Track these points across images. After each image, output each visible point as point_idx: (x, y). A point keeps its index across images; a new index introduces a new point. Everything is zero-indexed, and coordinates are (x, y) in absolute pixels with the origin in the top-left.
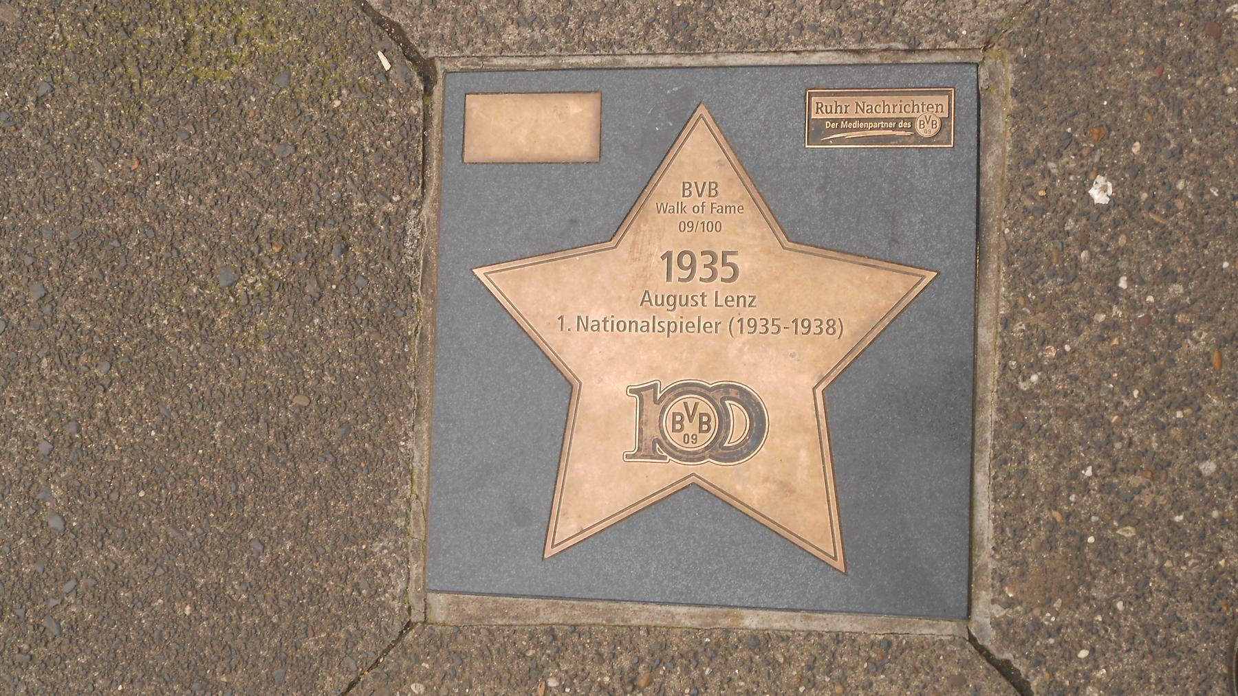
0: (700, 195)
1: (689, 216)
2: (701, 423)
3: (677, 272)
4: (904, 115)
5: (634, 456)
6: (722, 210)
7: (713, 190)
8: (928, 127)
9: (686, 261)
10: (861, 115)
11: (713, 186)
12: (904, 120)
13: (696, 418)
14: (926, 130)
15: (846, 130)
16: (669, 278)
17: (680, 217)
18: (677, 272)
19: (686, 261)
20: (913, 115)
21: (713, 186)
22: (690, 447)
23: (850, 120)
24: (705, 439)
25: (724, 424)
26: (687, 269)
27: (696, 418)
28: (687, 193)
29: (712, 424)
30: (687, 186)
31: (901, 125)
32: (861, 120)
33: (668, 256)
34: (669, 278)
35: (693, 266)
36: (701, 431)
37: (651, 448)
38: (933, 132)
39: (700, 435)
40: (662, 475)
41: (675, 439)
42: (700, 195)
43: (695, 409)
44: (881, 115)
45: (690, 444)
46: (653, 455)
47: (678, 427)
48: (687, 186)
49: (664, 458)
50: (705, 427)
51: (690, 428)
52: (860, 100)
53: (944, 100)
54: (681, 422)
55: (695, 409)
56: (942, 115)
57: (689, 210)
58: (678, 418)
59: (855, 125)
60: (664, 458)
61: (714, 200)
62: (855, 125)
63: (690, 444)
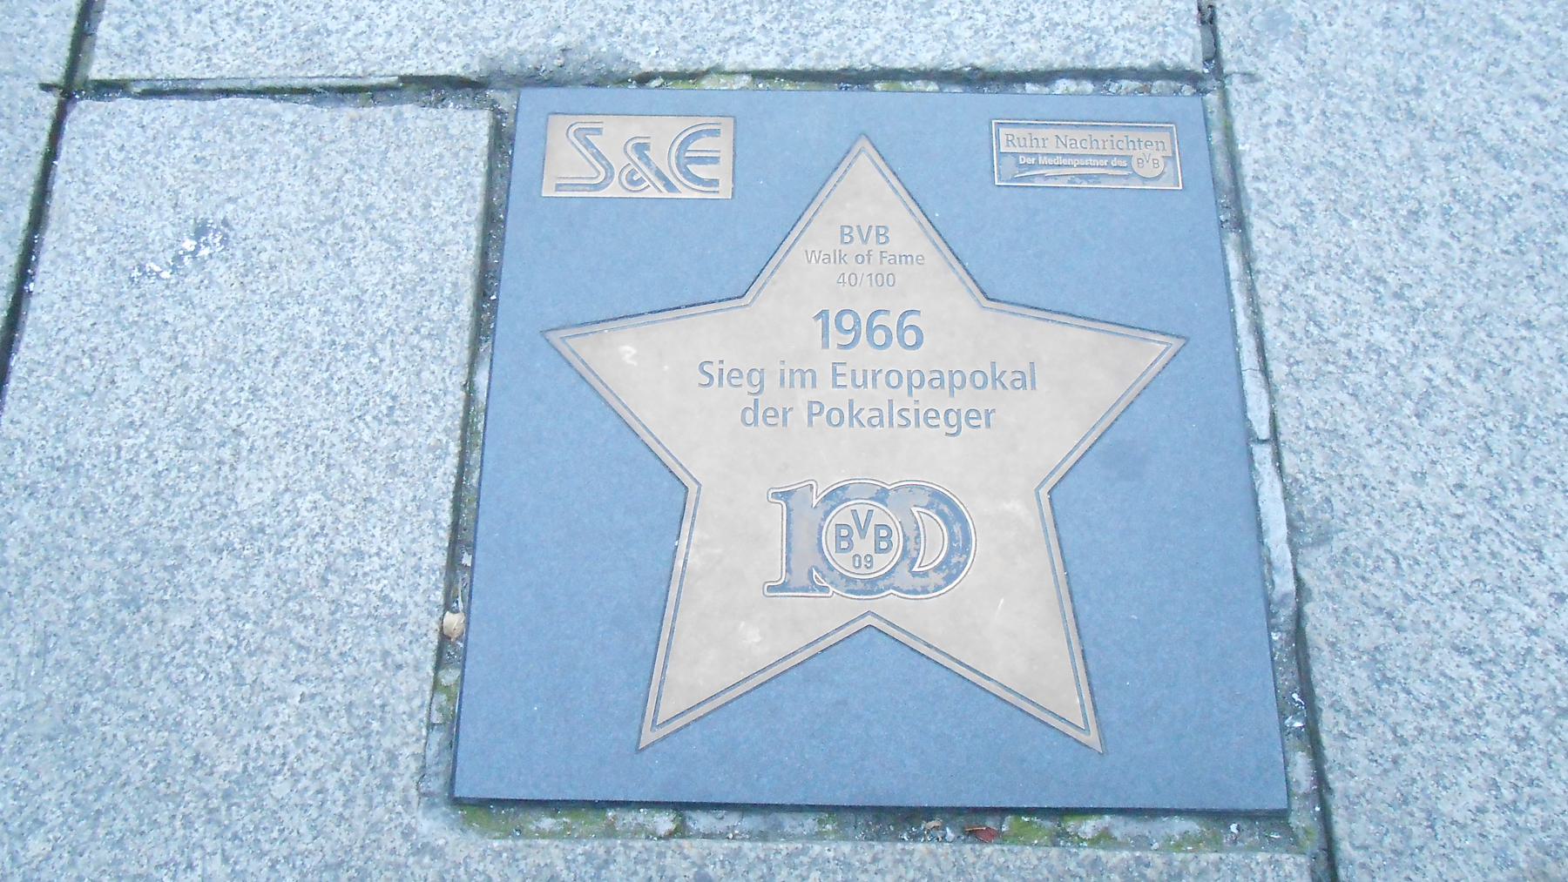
0: (865, 242)
2: (878, 539)
3: (835, 337)
5: (783, 587)
6: (894, 259)
7: (882, 233)
9: (848, 322)
11: (882, 231)
13: (871, 530)
16: (826, 345)
18: (835, 337)
19: (848, 322)
22: (863, 574)
24: (883, 563)
25: (913, 538)
26: (849, 331)
27: (871, 530)
28: (847, 239)
29: (894, 539)
30: (847, 231)
33: (823, 315)
34: (826, 345)
35: (856, 329)
36: (878, 550)
37: (800, 578)
39: (876, 557)
40: (829, 613)
41: (843, 562)
42: (865, 242)
43: (867, 521)
45: (863, 570)
46: (811, 587)
47: (844, 545)
48: (847, 231)
49: (823, 589)
50: (883, 545)
51: (864, 546)
54: (848, 538)
55: (867, 521)
57: (850, 259)
58: (844, 532)
60: (823, 589)
61: (883, 248)
63: (863, 570)
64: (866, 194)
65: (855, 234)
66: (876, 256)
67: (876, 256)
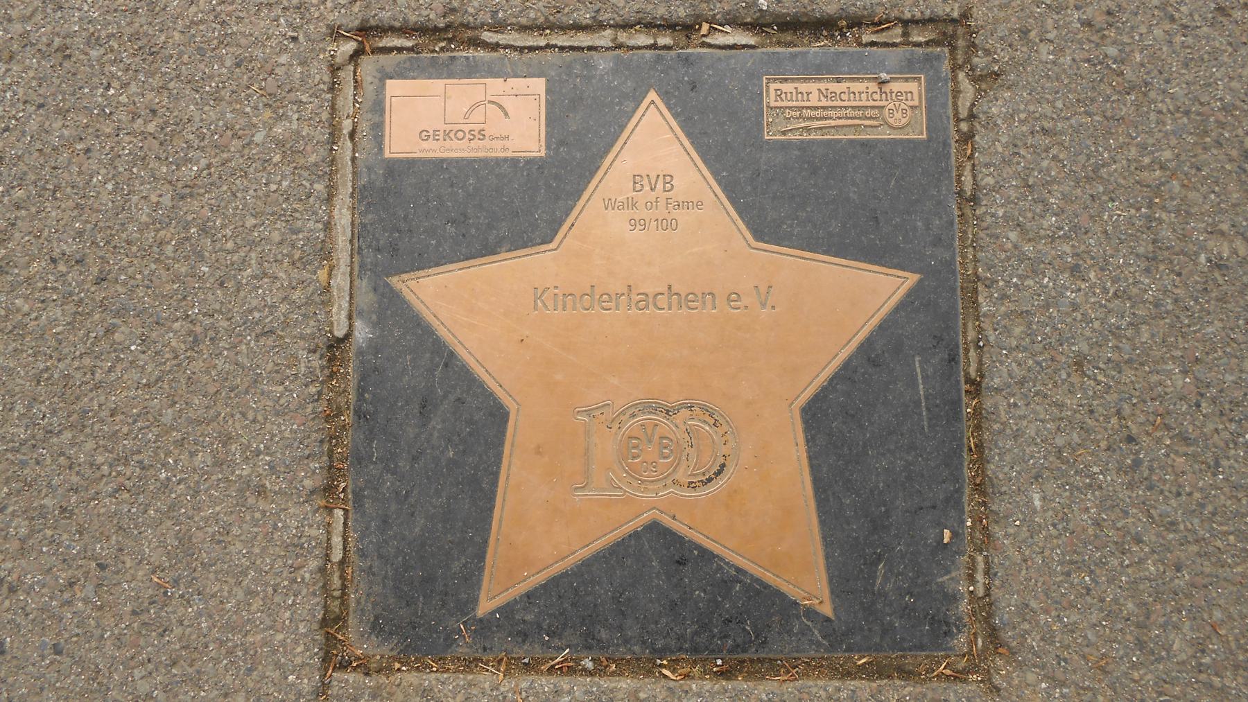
1: (641, 213)
4: (871, 103)
8: (898, 115)
10: (824, 103)
11: (668, 179)
12: (873, 107)
14: (898, 119)
15: (810, 119)
17: (628, 213)
20: (883, 103)
21: (668, 179)
23: (816, 108)
31: (869, 113)
32: (824, 108)
38: (904, 121)
44: (846, 104)
52: (823, 86)
53: (913, 86)
56: (911, 103)
57: (640, 205)
59: (819, 113)
62: (819, 113)
64: (653, 144)
65: (645, 182)
66: (662, 203)
67: (662, 203)
